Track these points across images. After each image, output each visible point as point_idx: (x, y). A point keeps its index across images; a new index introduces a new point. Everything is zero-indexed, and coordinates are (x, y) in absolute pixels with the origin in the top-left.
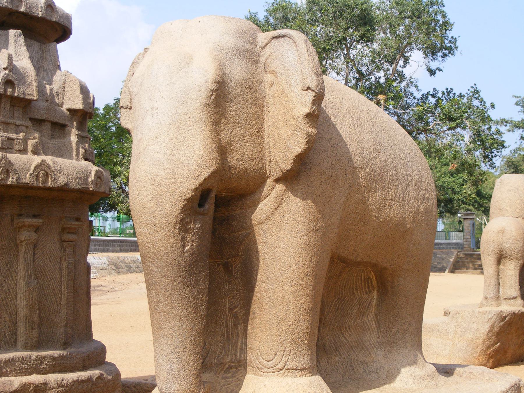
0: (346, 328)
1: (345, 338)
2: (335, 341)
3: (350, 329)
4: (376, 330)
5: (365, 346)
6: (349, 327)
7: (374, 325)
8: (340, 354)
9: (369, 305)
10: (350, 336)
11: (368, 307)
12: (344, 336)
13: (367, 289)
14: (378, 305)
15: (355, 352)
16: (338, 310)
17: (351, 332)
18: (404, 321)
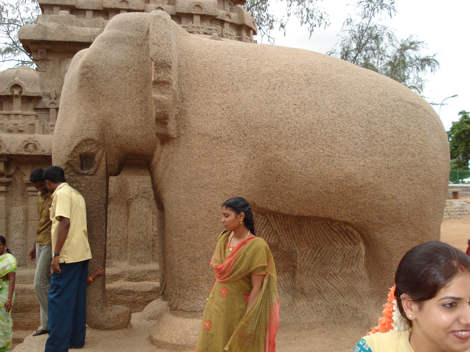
0: (330, 275)
1: (332, 284)
2: (317, 286)
3: (336, 276)
4: (368, 280)
5: (358, 293)
6: (334, 274)
7: (366, 275)
8: (324, 298)
9: (358, 255)
10: (338, 282)
11: (357, 258)
12: (329, 282)
13: (349, 241)
14: (366, 256)
15: (344, 297)
16: (316, 258)
17: (339, 279)
18: (390, 274)
